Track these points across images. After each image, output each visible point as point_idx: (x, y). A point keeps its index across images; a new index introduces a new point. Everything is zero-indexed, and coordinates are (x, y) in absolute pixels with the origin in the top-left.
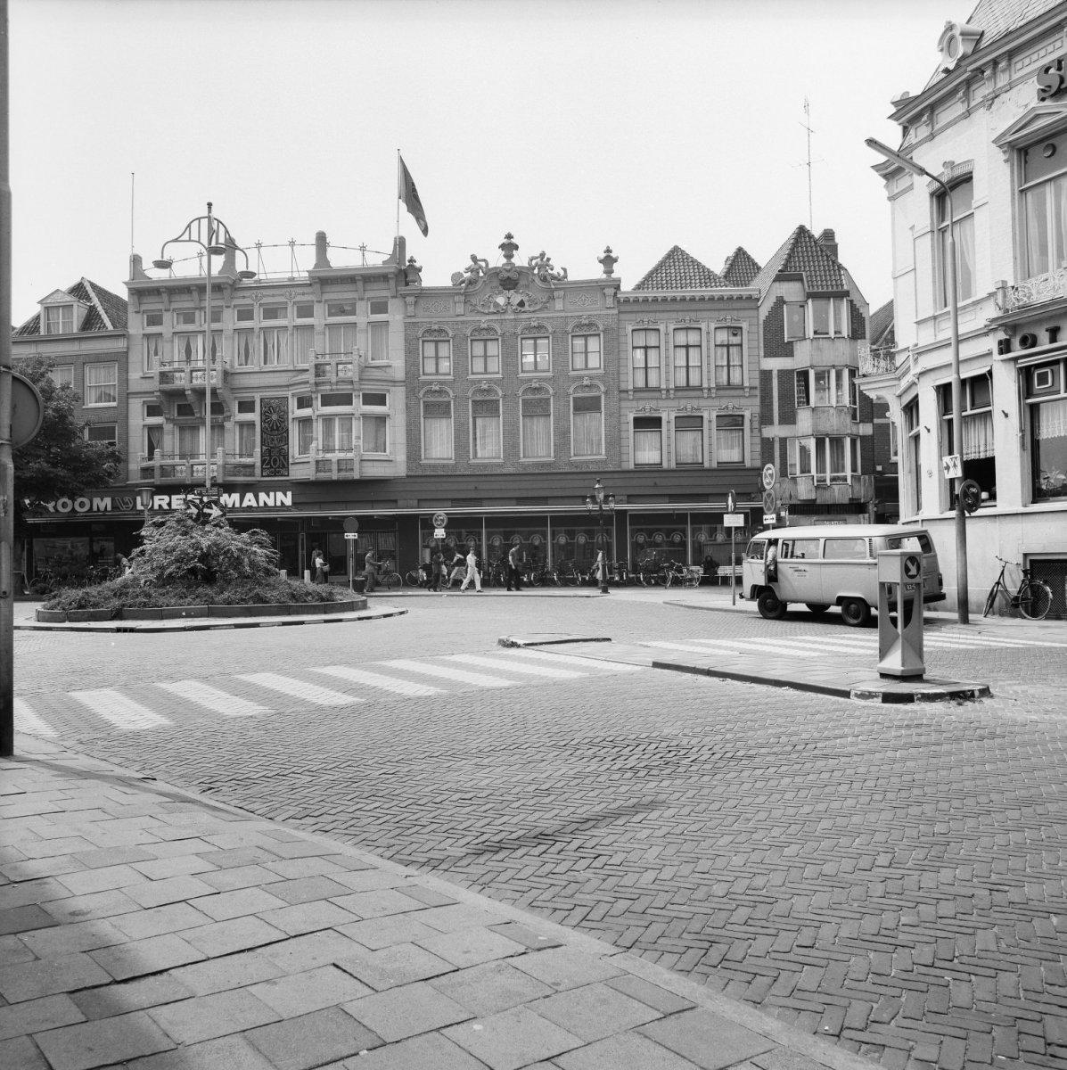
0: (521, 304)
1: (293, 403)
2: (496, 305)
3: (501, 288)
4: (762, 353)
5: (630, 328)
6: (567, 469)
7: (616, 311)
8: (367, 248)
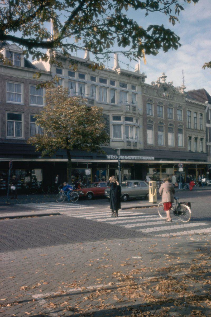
0: (168, 96)
1: (111, 118)
2: (163, 95)
3: (164, 90)
4: (206, 122)
5: (187, 110)
6: (177, 150)
7: (185, 104)
8: (130, 65)
